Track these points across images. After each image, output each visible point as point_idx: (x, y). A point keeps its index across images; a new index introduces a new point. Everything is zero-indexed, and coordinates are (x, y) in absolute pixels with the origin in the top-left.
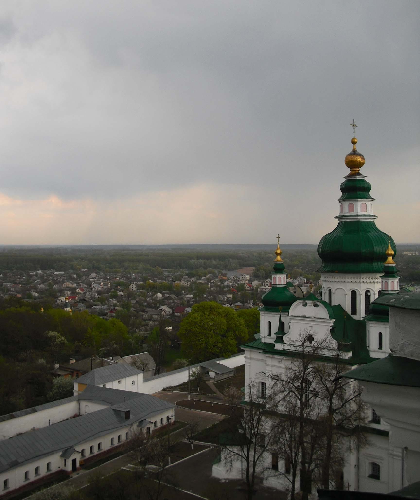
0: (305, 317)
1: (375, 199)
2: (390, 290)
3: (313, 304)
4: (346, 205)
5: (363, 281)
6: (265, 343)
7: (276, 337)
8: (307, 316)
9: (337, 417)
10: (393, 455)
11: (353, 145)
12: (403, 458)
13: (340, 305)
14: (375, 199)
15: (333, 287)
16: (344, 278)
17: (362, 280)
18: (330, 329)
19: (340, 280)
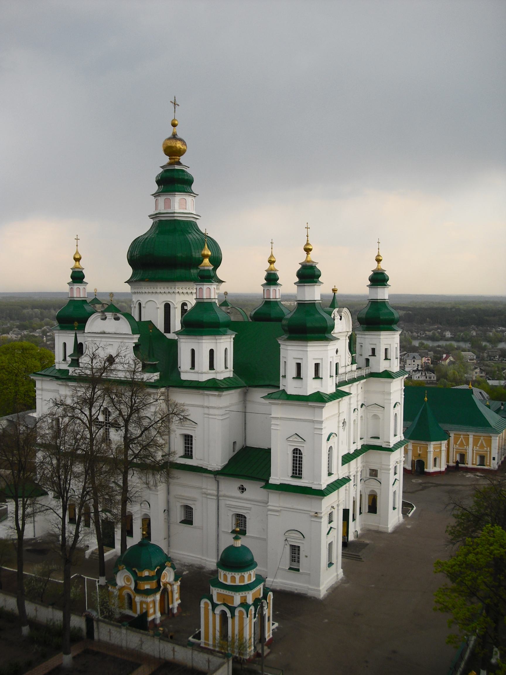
0: (105, 333)
1: (198, 195)
2: (205, 298)
3: (113, 317)
4: (161, 200)
5: (178, 292)
6: (60, 370)
7: (71, 360)
8: (106, 332)
9: (136, 449)
10: (207, 494)
11: (173, 127)
12: (218, 497)
13: (151, 321)
14: (198, 195)
15: (143, 299)
16: (155, 288)
17: (177, 291)
18: (133, 347)
19: (150, 291)
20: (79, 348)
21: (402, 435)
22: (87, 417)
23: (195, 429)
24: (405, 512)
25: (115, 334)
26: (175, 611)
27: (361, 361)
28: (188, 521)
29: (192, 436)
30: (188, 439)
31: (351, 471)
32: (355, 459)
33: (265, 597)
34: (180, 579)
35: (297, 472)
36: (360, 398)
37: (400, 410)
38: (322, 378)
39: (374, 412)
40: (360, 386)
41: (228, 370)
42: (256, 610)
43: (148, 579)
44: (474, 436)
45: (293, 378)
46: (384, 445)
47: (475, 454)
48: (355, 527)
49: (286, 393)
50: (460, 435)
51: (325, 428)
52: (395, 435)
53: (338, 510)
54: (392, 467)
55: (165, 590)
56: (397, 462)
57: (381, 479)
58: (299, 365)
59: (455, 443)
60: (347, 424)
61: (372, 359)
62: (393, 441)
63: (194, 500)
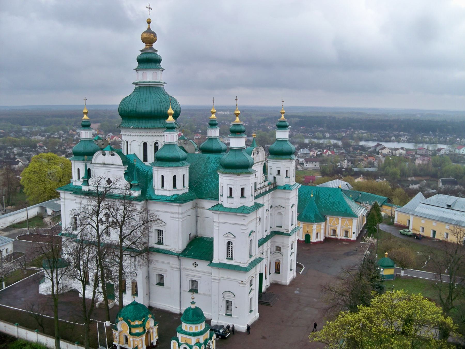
0: (104, 164)
4: (140, 73)
6: (76, 186)
12: (180, 270)
15: (129, 139)
19: (134, 134)
20: (88, 173)
21: (297, 224)
22: (96, 223)
23: (164, 226)
24: (297, 271)
25: (112, 165)
26: (155, 344)
27: (271, 179)
28: (161, 283)
29: (162, 231)
30: (160, 232)
31: (264, 249)
32: (266, 242)
33: (211, 338)
34: (157, 324)
35: (230, 255)
36: (269, 202)
37: (295, 209)
38: (246, 197)
39: (279, 210)
40: (270, 195)
41: (185, 188)
42: (205, 347)
43: (136, 326)
44: (342, 218)
45: (228, 197)
46: (285, 232)
47: (342, 230)
48: (267, 284)
49: (223, 206)
50: (333, 218)
51: (247, 229)
52: (292, 225)
53: (256, 277)
54: (290, 245)
55: (148, 332)
56: (293, 241)
57: (283, 253)
58: (231, 189)
59: (330, 223)
60: (262, 219)
61: (277, 177)
62: (291, 228)
63: (166, 271)
